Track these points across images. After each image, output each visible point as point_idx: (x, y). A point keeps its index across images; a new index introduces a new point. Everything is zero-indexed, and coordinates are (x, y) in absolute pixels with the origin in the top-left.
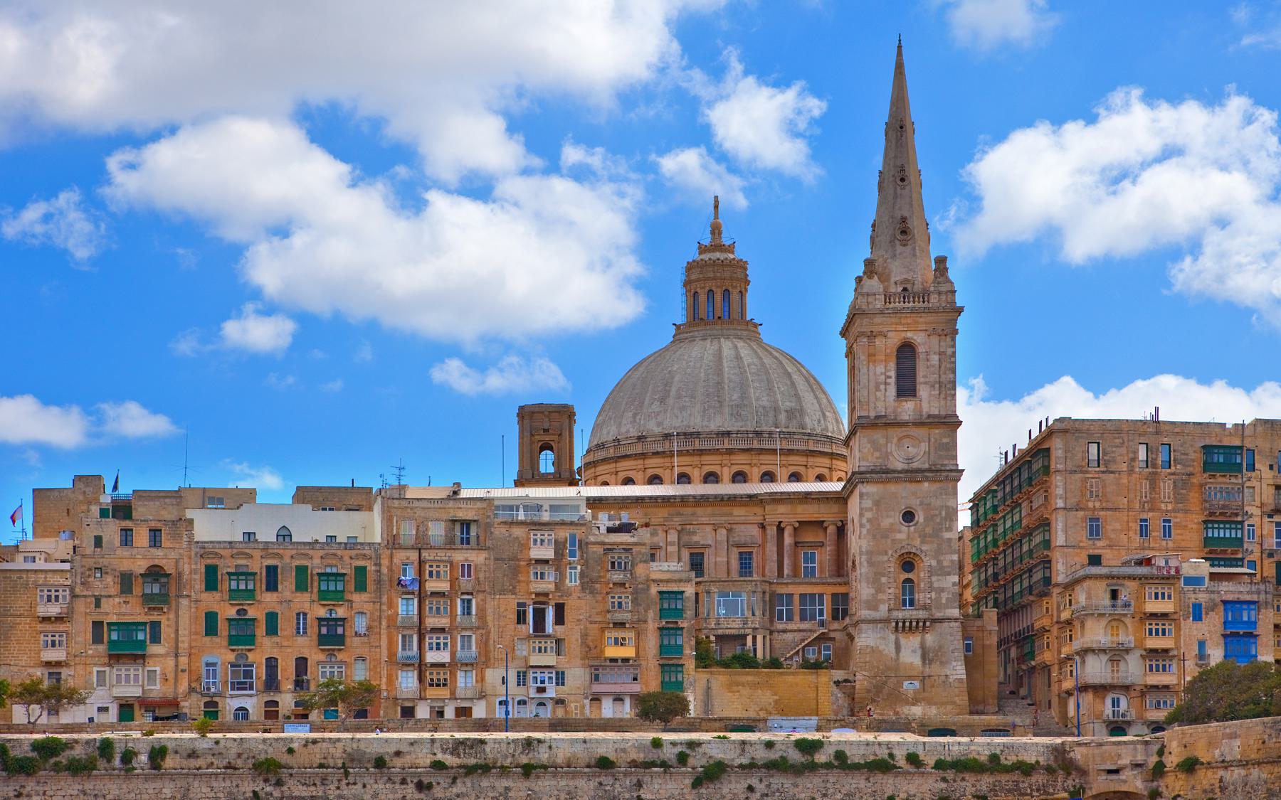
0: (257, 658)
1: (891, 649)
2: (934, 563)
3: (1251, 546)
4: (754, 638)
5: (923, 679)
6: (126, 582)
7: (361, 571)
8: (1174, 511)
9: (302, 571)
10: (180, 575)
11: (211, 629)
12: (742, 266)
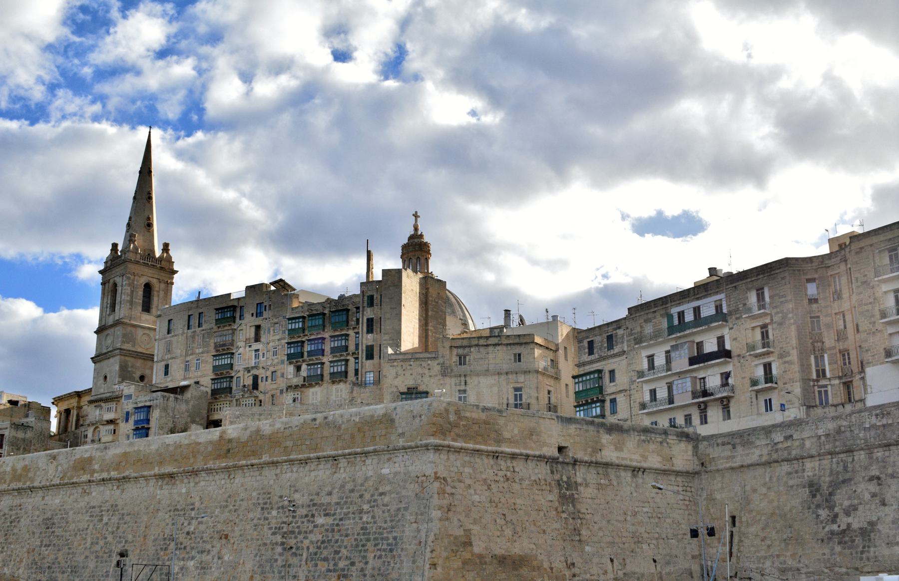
8: (202, 353)
12: (426, 245)
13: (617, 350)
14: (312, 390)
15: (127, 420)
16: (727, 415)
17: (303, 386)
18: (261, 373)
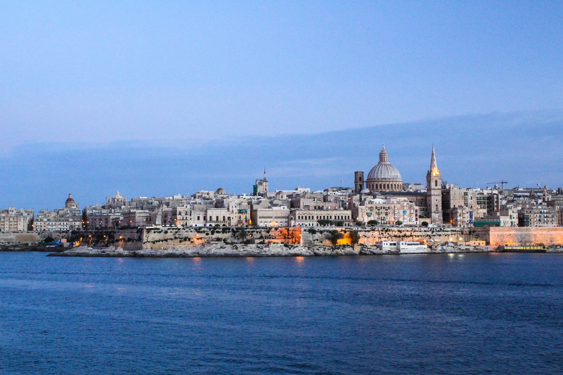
0: (380, 217)
3: (469, 203)
7: (389, 207)
9: (384, 207)
11: (376, 214)
16: (547, 224)
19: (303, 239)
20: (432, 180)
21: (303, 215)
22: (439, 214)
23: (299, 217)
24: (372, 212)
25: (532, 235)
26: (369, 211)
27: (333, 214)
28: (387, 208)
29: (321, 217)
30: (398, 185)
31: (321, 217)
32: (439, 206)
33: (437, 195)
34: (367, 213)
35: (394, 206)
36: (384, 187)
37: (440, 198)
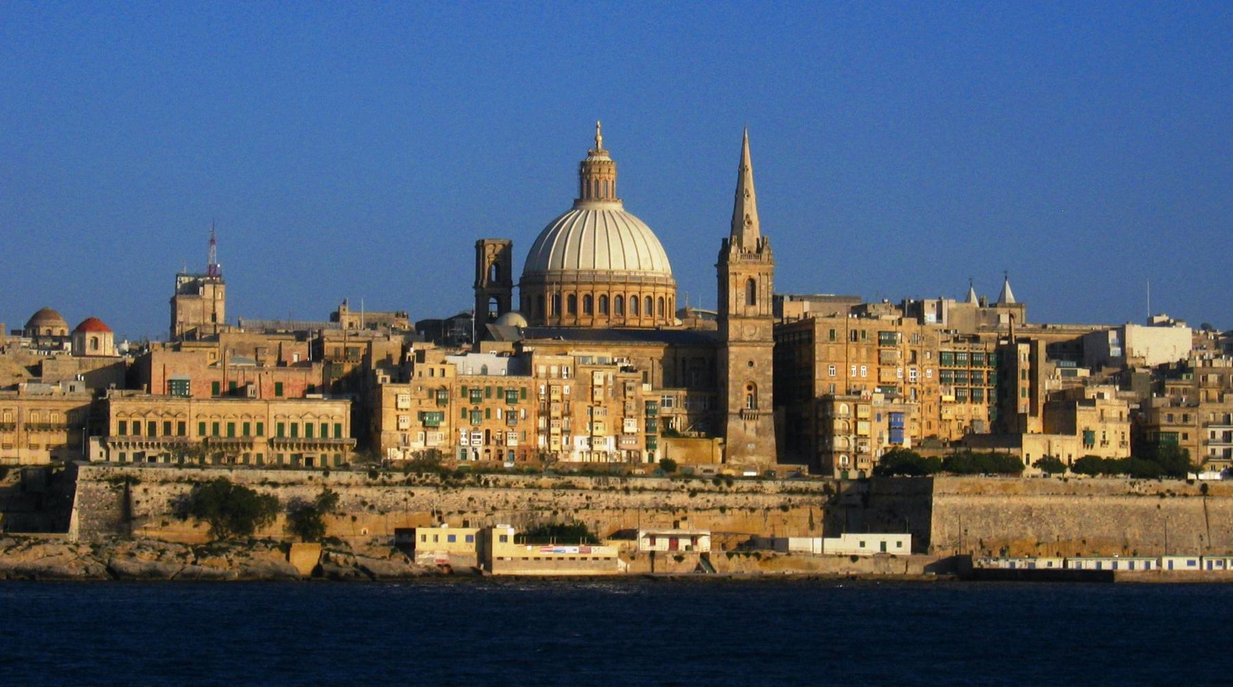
1: (741, 428)
2: (762, 387)
4: (676, 419)
5: (757, 443)
6: (431, 393)
7: (524, 390)
10: (451, 390)
11: (464, 416)
13: (1190, 423)
14: (958, 406)
15: (879, 420)
17: (955, 402)
18: (918, 386)
19: (82, 511)
20: (731, 277)
21: (142, 420)
22: (759, 423)
23: (123, 426)
24: (446, 410)
25: (1132, 514)
26: (429, 406)
27: (272, 414)
28: (478, 390)
29: (216, 426)
30: (661, 298)
31: (216, 426)
32: (760, 386)
33: (753, 343)
34: (422, 415)
35: (549, 386)
36: (589, 309)
37: (765, 354)
